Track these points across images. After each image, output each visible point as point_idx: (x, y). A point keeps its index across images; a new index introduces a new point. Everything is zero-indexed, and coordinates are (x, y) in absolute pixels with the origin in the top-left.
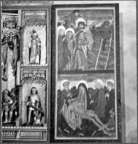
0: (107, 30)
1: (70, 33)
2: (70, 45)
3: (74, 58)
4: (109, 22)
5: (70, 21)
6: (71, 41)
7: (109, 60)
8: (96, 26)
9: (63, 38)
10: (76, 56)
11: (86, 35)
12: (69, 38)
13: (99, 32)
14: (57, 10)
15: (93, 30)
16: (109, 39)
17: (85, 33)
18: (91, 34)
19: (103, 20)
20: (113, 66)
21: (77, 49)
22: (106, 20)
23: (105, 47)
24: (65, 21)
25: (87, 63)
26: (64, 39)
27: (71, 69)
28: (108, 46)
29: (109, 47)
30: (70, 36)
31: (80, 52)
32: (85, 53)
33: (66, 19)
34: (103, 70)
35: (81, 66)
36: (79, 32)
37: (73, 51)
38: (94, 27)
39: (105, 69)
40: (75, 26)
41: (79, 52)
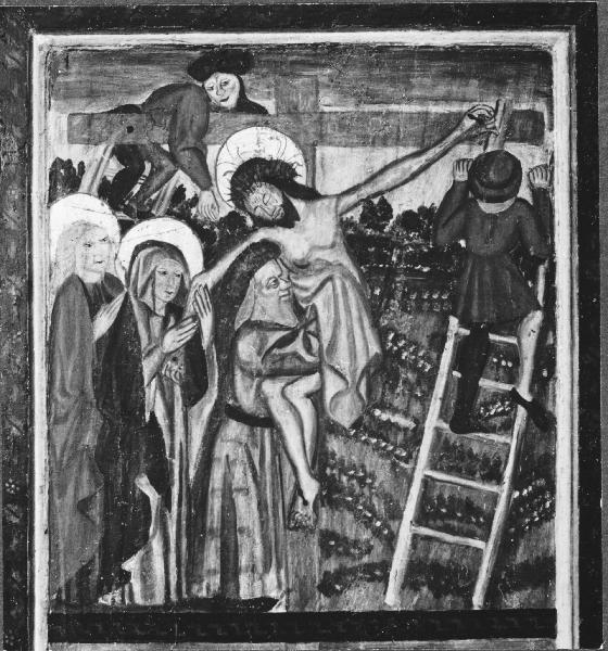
0: (497, 244)
1: (165, 264)
2: (157, 374)
3: (197, 496)
4: (517, 164)
5: (166, 147)
6: (173, 340)
7: (512, 517)
8: (404, 201)
9: (94, 312)
10: (217, 474)
11: (301, 283)
12: (149, 312)
13: (424, 259)
15: (369, 236)
16: (512, 325)
17: (302, 267)
18: (356, 274)
19: (459, 141)
20: (543, 571)
21: (229, 410)
22: (489, 150)
23: (480, 400)
24: (120, 152)
25: (315, 539)
26: (103, 323)
27: (173, 597)
28: (508, 387)
29: (514, 398)
30: (163, 295)
31: (252, 435)
32: (296, 445)
33: (130, 129)
34: (461, 607)
35: (260, 568)
36: (246, 252)
37: (186, 432)
38: (377, 211)
39: (477, 601)
40: (206, 198)
41: (244, 439)
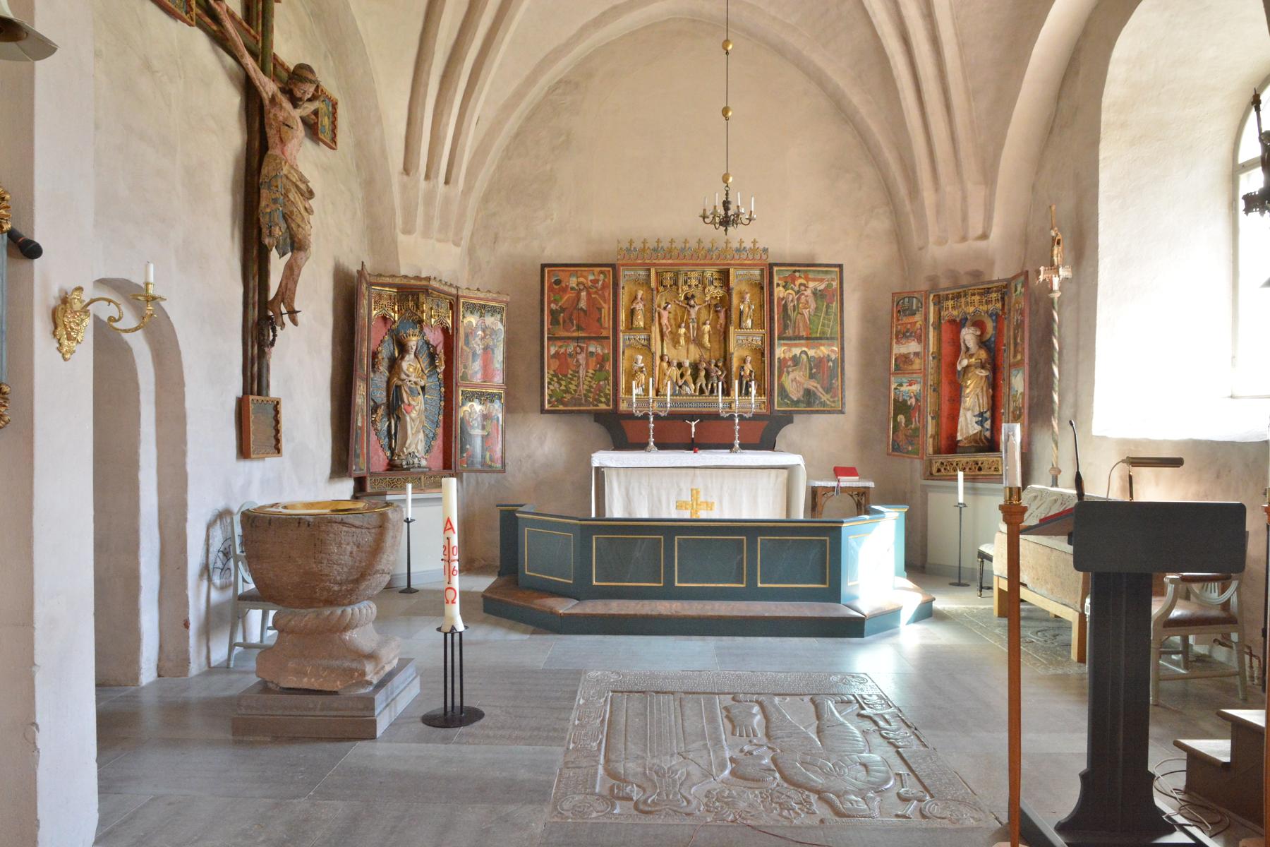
14: (775, 269)
15: (815, 293)
37: (793, 315)
